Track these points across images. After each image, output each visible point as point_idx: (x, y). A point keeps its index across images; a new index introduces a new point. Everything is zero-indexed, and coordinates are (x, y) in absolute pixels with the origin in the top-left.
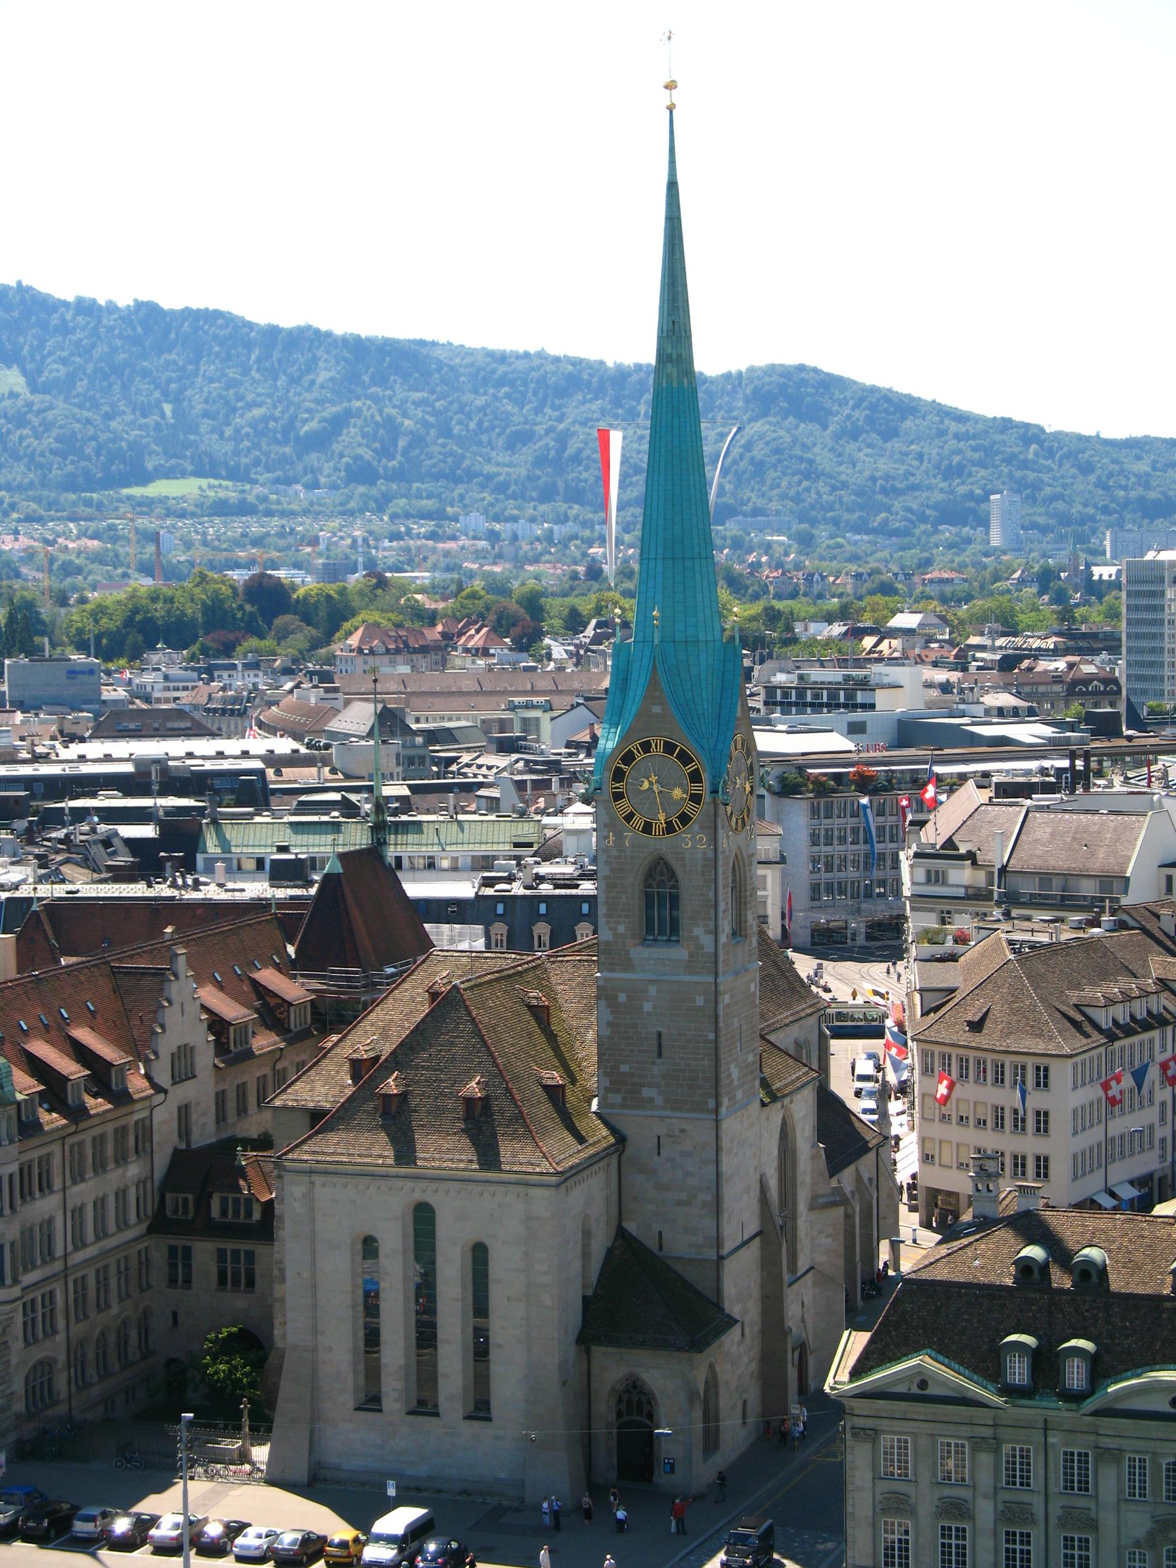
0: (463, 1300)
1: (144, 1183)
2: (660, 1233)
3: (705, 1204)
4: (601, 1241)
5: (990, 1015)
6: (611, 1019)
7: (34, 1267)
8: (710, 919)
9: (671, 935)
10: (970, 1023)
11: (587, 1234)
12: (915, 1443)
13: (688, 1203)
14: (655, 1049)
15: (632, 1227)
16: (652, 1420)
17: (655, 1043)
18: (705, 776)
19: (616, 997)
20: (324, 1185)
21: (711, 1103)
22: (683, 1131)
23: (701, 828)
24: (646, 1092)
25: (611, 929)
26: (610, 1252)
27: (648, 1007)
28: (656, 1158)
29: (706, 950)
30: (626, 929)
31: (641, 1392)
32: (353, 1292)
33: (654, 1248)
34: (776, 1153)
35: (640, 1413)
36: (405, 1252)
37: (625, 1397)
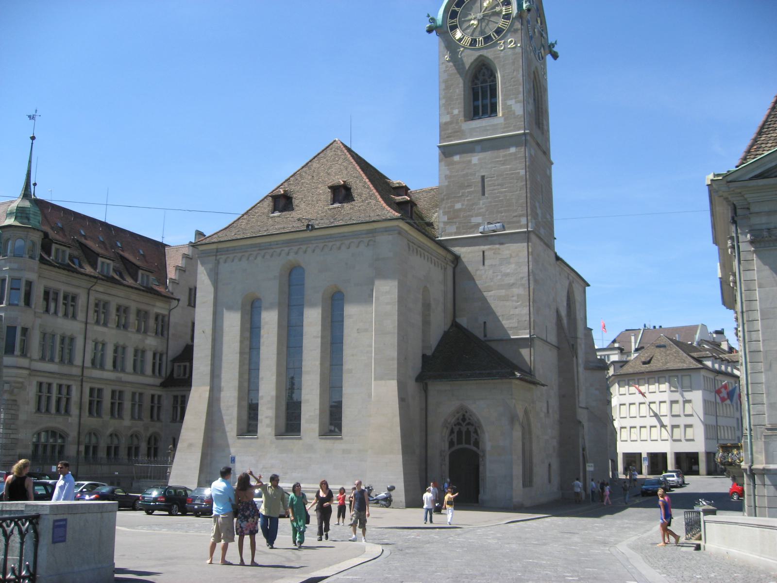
0: (323, 337)
1: (161, 355)
2: (485, 323)
3: (518, 296)
4: (439, 324)
5: (653, 359)
6: (448, 173)
7: (52, 360)
9: (491, 114)
10: (644, 363)
11: (427, 307)
13: (505, 298)
14: (480, 189)
15: (463, 321)
16: (478, 448)
17: (480, 185)
20: (225, 262)
21: (524, 221)
24: (475, 220)
25: (448, 113)
26: (446, 335)
28: (481, 267)
29: (517, 114)
30: (459, 112)
31: (469, 424)
32: (241, 342)
33: (481, 336)
34: (565, 304)
35: (468, 442)
37: (456, 429)
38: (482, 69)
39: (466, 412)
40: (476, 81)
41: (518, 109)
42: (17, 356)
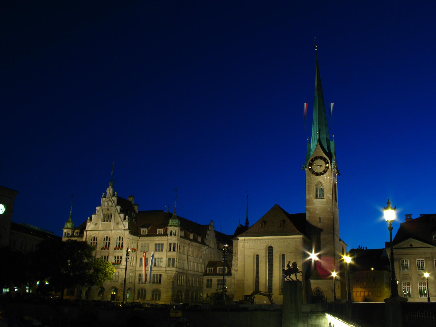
6: (309, 215)
8: (331, 192)
12: (410, 261)
17: (319, 220)
18: (329, 162)
19: (310, 210)
21: (332, 231)
22: (326, 238)
23: (328, 173)
25: (309, 196)
27: (317, 212)
29: (330, 198)
30: (312, 196)
31: (320, 292)
32: (253, 267)
36: (266, 256)
38: (319, 182)
39: (319, 288)
40: (317, 186)
41: (331, 197)
42: (171, 267)
